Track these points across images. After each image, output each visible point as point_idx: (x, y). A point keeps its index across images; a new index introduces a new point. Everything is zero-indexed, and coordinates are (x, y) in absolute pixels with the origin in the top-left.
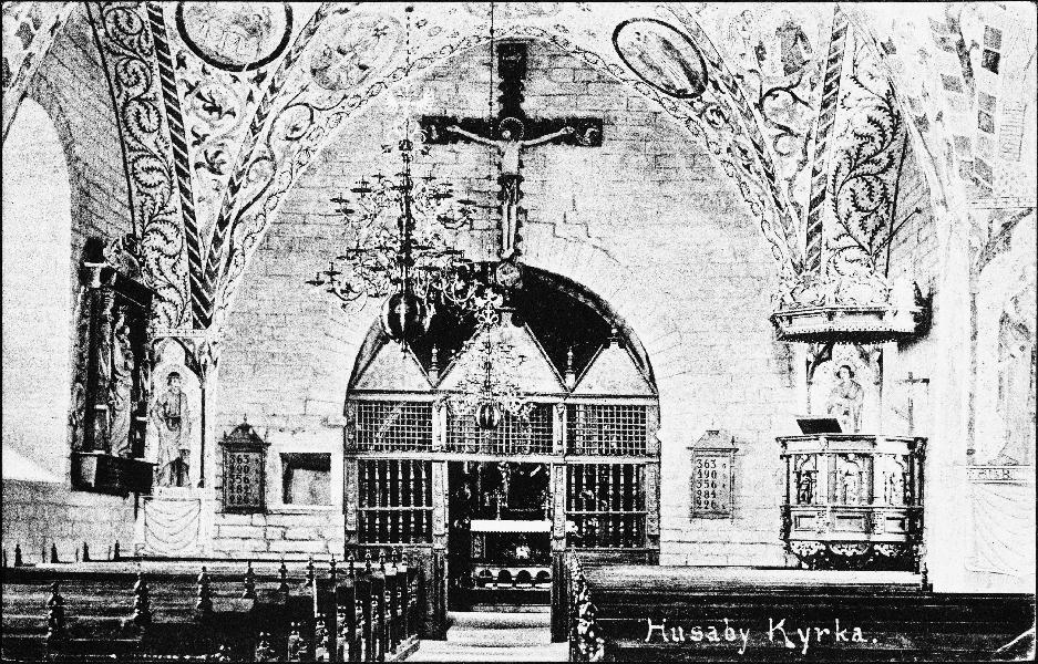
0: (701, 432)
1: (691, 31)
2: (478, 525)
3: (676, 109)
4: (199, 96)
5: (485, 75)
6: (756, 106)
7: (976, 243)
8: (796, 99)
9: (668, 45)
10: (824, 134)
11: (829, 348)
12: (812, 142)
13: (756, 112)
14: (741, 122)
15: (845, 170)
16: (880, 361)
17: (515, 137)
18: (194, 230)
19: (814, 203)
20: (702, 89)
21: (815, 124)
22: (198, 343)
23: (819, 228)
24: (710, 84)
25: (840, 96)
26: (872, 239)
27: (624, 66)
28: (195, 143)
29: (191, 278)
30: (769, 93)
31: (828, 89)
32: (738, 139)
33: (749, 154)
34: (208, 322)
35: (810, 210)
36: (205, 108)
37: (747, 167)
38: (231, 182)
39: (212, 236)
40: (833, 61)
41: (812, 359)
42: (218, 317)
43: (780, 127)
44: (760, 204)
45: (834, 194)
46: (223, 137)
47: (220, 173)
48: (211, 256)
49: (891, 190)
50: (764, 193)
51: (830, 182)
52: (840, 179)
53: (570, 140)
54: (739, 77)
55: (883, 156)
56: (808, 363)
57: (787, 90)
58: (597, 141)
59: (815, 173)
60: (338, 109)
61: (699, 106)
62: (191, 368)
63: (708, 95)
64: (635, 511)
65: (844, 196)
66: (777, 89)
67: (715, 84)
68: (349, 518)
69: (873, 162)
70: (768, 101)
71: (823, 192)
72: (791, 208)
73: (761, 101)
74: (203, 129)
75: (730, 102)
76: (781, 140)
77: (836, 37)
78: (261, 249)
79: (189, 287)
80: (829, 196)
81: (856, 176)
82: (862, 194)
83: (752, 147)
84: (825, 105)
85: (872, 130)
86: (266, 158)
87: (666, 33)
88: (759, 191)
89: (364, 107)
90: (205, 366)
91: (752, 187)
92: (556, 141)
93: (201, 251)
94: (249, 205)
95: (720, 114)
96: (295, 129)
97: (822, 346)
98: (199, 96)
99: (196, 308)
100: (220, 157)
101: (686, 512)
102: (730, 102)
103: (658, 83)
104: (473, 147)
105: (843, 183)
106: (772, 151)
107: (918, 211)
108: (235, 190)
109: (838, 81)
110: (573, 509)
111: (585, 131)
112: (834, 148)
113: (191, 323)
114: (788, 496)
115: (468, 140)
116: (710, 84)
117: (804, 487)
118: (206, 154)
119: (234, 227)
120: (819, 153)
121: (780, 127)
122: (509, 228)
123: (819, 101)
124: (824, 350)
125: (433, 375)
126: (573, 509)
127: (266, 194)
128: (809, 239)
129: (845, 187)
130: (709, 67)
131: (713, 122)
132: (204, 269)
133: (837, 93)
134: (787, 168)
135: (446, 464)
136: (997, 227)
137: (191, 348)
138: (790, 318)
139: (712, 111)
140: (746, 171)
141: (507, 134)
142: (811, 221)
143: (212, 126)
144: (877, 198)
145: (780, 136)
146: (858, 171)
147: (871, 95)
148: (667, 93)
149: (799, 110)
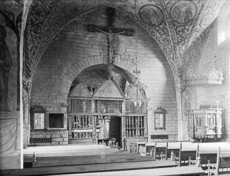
0: (156, 108)
1: (163, 9)
2: (75, 131)
3: (150, 29)
4: (35, 11)
5: (104, 16)
6: (175, 29)
8: (185, 28)
9: (155, 12)
10: (190, 38)
12: (187, 39)
13: (175, 31)
14: (170, 33)
15: (192, 47)
16: (196, 91)
17: (112, 33)
18: (28, 49)
19: (184, 54)
20: (160, 24)
21: (188, 35)
22: (27, 82)
23: (185, 60)
24: (163, 23)
25: (196, 29)
26: (195, 63)
27: (139, 17)
28: (30, 24)
29: (26, 63)
30: (179, 27)
32: (169, 37)
33: (170, 41)
34: (30, 76)
35: (183, 55)
36: (35, 14)
37: (168, 45)
38: (40, 36)
39: (33, 51)
41: (181, 91)
42: (32, 75)
43: (180, 35)
44: (169, 53)
45: (189, 52)
46: (39, 23)
47: (37, 33)
48: (32, 57)
49: (201, 52)
50: (172, 51)
51: (189, 49)
52: (191, 49)
53: (127, 35)
54: (172, 22)
55: (201, 44)
56: (181, 92)
57: (184, 26)
58: (131, 35)
59: (186, 47)
60: (66, 20)
61: (157, 28)
62: (25, 89)
63: (161, 26)
64: (130, 128)
65: (191, 53)
66: (180, 26)
67: (165, 24)
68: (70, 132)
69: (198, 45)
70: (178, 28)
71: (187, 52)
72: (179, 56)
73: (177, 27)
74: (34, 20)
75: (168, 28)
76: (180, 38)
77: (199, 14)
78: (43, 56)
79: (25, 66)
80: (188, 52)
81: (194, 48)
82: (195, 53)
83: (171, 39)
84: (192, 31)
85: (200, 37)
86: (49, 31)
87: (155, 8)
88: (170, 50)
89: (72, 20)
90: (29, 89)
91: (168, 49)
92: (120, 34)
93: (29, 56)
94: (43, 43)
95: (163, 31)
96: (57, 24)
98: (34, 10)
99: (27, 72)
100: (38, 29)
101: (154, 128)
102: (168, 28)
103: (147, 22)
104: (101, 34)
105: (191, 50)
106: (176, 41)
107: (215, 57)
108: (40, 39)
109: (196, 25)
110: (127, 128)
111: (129, 33)
113: (25, 76)
114: (194, 124)
115: (101, 32)
116: (163, 23)
117: (199, 122)
118: (34, 28)
119: (38, 50)
121: (180, 35)
122: (111, 54)
123: (190, 29)
125: (92, 93)
126: (127, 128)
127: (47, 41)
128: (182, 62)
130: (165, 18)
131: (161, 33)
132: (30, 61)
133: (195, 28)
134: (179, 45)
135: (96, 116)
137: (25, 84)
138: (195, 80)
139: (161, 30)
140: (167, 46)
141: (110, 31)
142: (183, 58)
143: (37, 20)
144: (198, 53)
145: (179, 37)
146: (195, 47)
147: (202, 29)
148: (148, 25)
149: (185, 31)
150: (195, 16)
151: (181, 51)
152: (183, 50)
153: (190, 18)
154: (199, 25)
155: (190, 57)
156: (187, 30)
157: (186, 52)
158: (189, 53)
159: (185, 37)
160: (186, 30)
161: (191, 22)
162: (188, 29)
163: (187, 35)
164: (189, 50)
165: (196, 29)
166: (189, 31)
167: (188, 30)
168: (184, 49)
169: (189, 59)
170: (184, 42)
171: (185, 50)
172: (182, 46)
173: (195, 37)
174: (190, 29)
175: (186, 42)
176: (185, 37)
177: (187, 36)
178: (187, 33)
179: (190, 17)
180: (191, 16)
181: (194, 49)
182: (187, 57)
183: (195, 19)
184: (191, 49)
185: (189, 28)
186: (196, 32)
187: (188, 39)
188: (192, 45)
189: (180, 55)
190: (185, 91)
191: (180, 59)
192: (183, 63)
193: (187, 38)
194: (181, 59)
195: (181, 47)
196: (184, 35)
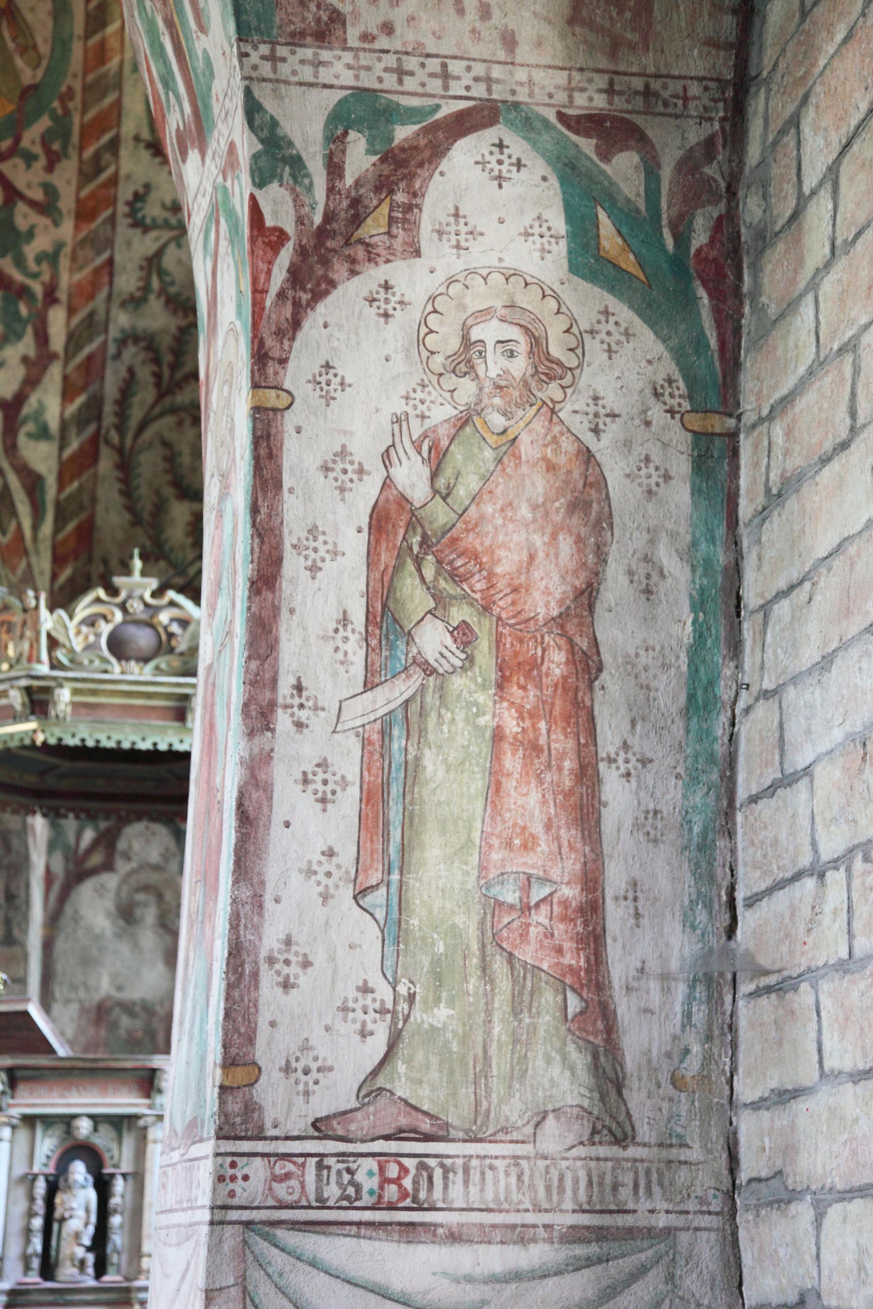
7: (279, 210)
11: (107, 841)
15: (144, 397)
19: (67, 471)
21: (64, 263)
25: (125, 193)
31: (86, 175)
35: (61, 488)
40: (95, 90)
45: (120, 451)
52: (136, 414)
71: (94, 442)
97: (89, 835)
105: (142, 427)
109: (114, 145)
112: (114, 332)
120: (74, 341)
123: (67, 203)
124: (96, 844)
129: (147, 435)
133: (114, 181)
136: (359, 159)
142: (60, 520)
150: (61, 43)
151: (22, 439)
152: (43, 433)
153: (28, 76)
154: (145, 155)
155: (146, 507)
156: (33, 204)
157: (74, 445)
158: (125, 466)
159: (38, 289)
160: (21, 208)
161: (44, 123)
162: (37, 195)
163: (52, 258)
164: (121, 429)
165: (125, 193)
166: (56, 224)
167: (47, 207)
168: (54, 425)
169: (137, 521)
170: (42, 338)
171: (64, 426)
172: (31, 382)
173: (146, 289)
174: (67, 203)
175: (58, 341)
176: (38, 289)
177: (55, 277)
178: (41, 243)
179: (19, 62)
180: (28, 48)
181: (170, 420)
182: (109, 494)
183: (78, 86)
184: (136, 414)
185: (50, 191)
186: (140, 225)
187: (71, 311)
188: (131, 371)
189: (34, 484)
190: (108, 866)
191: (36, 527)
192: (66, 573)
193: (62, 295)
194: (47, 527)
195: (20, 398)
196: (20, 262)
